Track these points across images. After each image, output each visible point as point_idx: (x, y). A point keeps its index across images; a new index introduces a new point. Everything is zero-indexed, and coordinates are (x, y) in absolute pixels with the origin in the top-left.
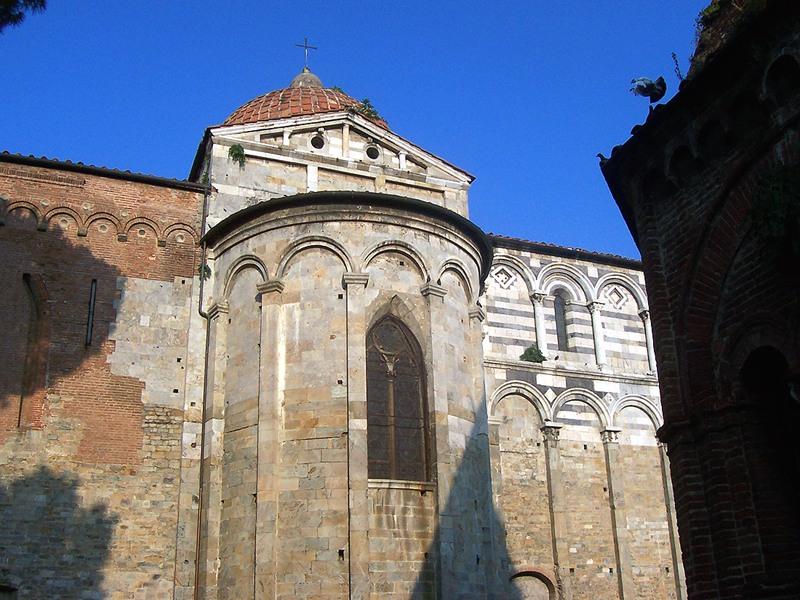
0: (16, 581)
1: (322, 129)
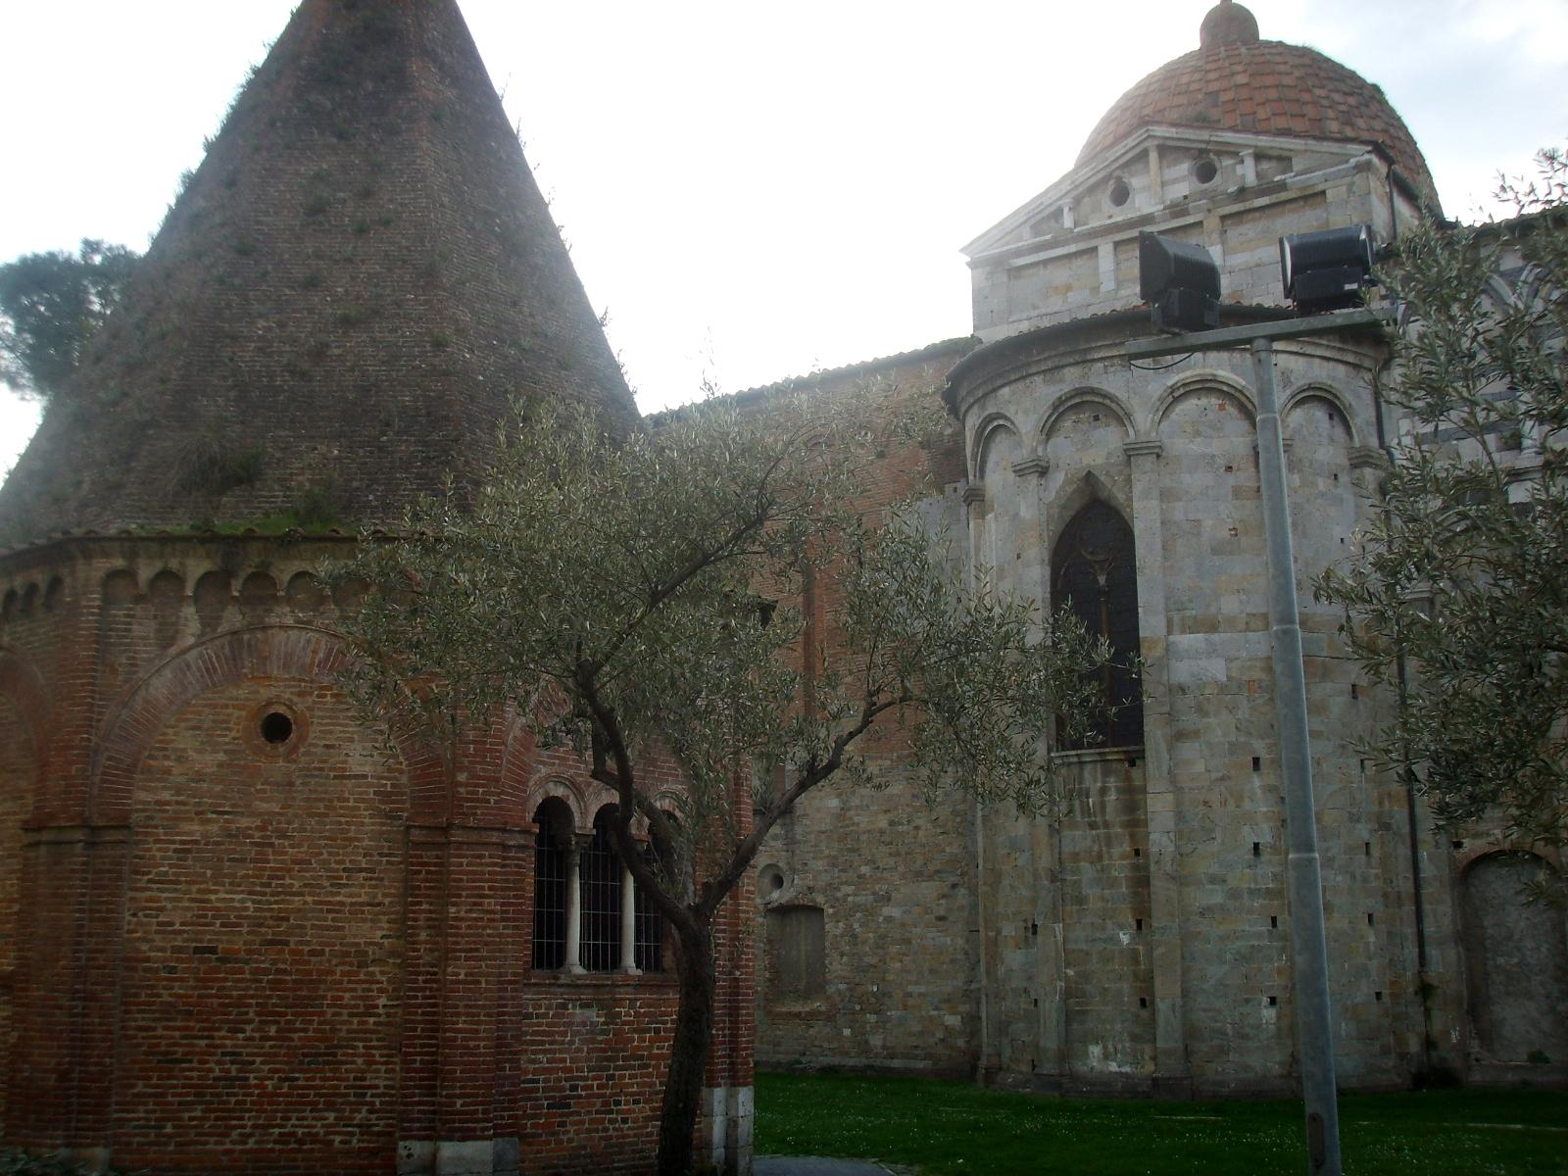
0: (820, 899)
1: (1117, 173)
